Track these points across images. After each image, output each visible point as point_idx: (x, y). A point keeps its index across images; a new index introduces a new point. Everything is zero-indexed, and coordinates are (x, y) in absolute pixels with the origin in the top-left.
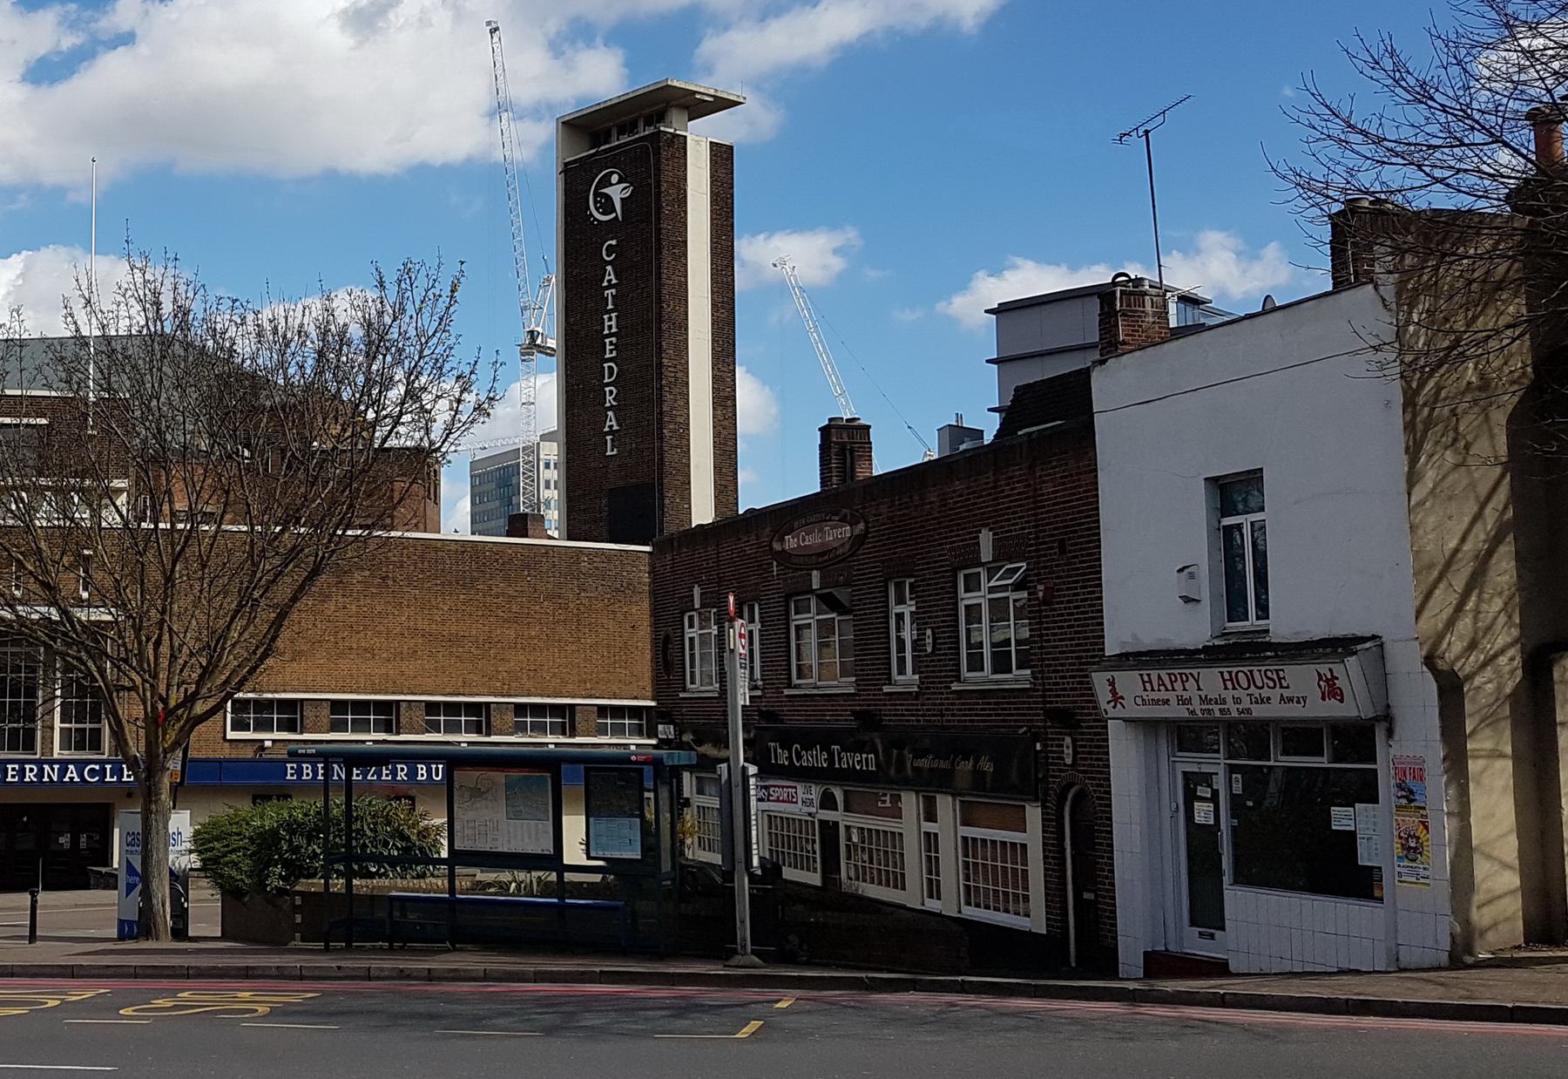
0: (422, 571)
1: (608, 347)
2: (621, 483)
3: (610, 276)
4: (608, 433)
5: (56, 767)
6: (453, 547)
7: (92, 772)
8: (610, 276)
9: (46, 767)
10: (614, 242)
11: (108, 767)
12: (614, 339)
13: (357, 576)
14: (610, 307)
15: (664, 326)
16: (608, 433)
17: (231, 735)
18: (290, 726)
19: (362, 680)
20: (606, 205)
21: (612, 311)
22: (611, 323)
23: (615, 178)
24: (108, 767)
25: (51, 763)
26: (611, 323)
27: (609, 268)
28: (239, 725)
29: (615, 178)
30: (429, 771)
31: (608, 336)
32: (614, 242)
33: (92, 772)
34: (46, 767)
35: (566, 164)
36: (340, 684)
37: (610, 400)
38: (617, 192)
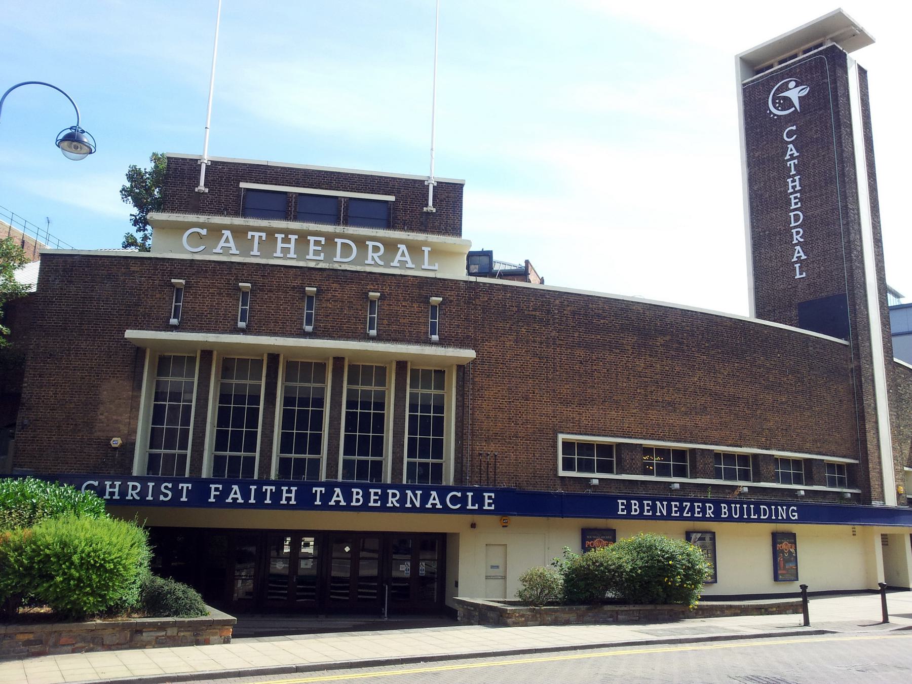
0: (708, 341)
1: (793, 201)
2: (811, 298)
3: (792, 150)
4: (796, 262)
5: (419, 493)
6: (729, 324)
7: (454, 500)
8: (792, 150)
9: (409, 493)
10: (794, 128)
11: (470, 494)
12: (798, 195)
13: (660, 340)
14: (793, 172)
15: (847, 180)
16: (796, 262)
17: (562, 473)
18: (605, 467)
19: (667, 429)
20: (788, 103)
21: (795, 175)
22: (794, 184)
23: (792, 84)
24: (470, 494)
25: (413, 489)
26: (794, 184)
27: (791, 146)
28: (568, 466)
29: (792, 84)
30: (730, 510)
31: (791, 194)
32: (794, 128)
33: (454, 500)
34: (409, 493)
35: (744, 85)
36: (651, 431)
37: (797, 238)
38: (795, 93)
